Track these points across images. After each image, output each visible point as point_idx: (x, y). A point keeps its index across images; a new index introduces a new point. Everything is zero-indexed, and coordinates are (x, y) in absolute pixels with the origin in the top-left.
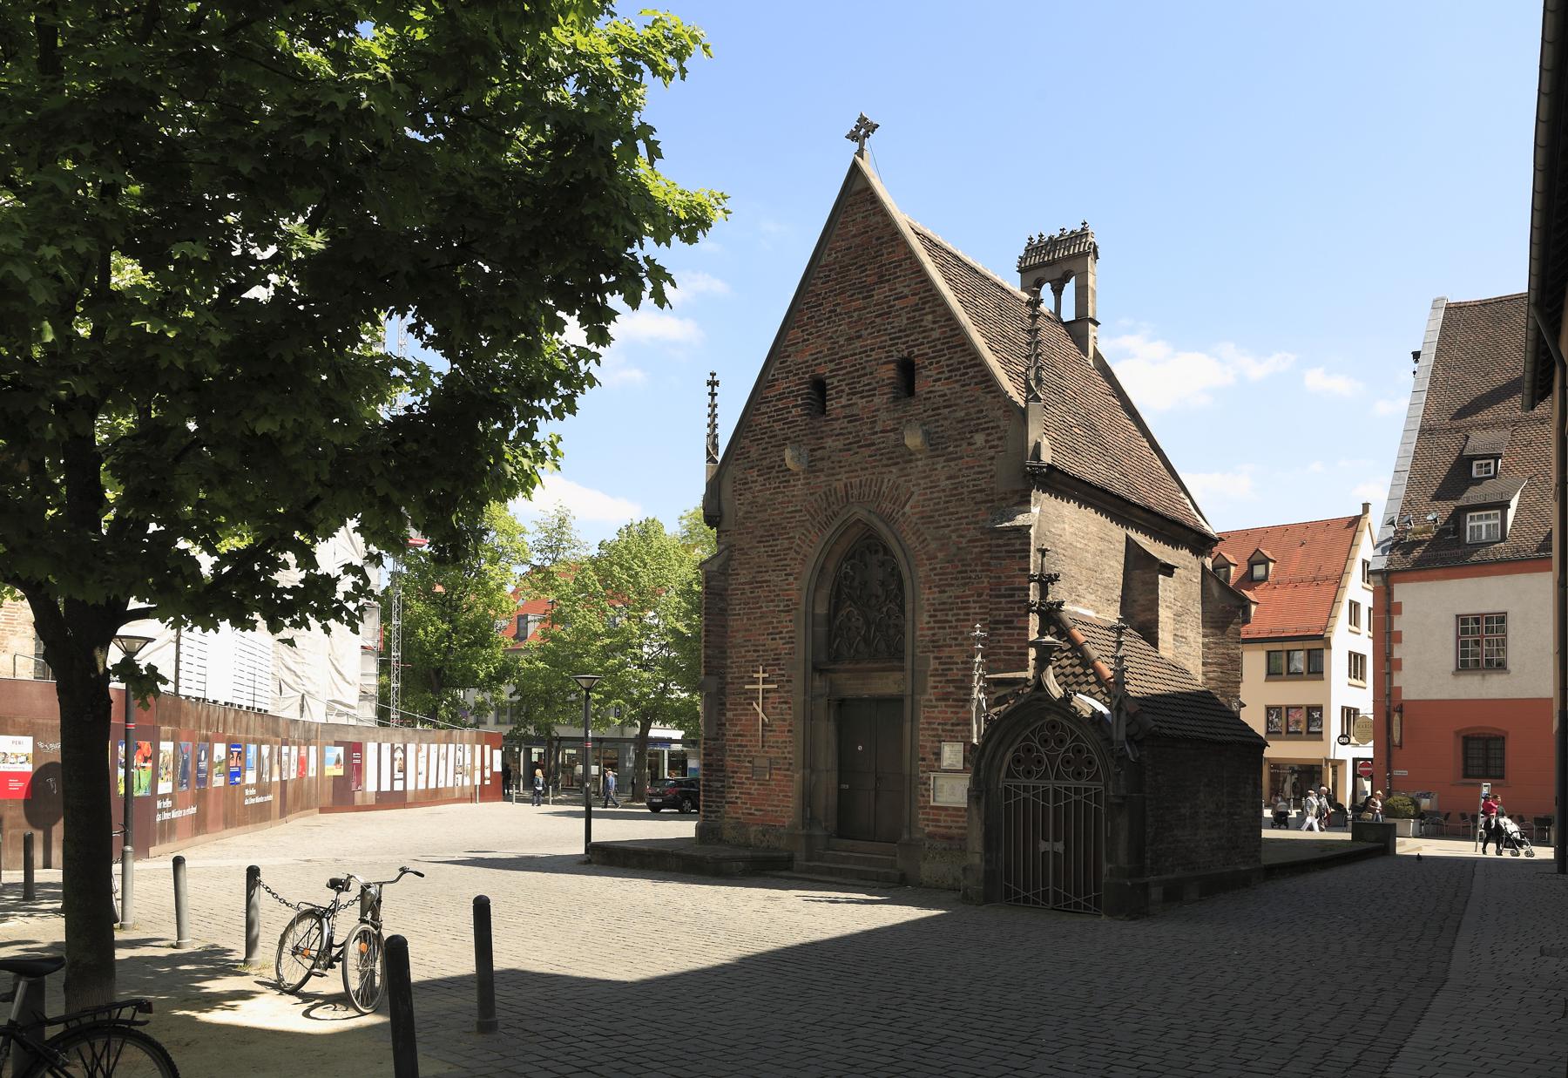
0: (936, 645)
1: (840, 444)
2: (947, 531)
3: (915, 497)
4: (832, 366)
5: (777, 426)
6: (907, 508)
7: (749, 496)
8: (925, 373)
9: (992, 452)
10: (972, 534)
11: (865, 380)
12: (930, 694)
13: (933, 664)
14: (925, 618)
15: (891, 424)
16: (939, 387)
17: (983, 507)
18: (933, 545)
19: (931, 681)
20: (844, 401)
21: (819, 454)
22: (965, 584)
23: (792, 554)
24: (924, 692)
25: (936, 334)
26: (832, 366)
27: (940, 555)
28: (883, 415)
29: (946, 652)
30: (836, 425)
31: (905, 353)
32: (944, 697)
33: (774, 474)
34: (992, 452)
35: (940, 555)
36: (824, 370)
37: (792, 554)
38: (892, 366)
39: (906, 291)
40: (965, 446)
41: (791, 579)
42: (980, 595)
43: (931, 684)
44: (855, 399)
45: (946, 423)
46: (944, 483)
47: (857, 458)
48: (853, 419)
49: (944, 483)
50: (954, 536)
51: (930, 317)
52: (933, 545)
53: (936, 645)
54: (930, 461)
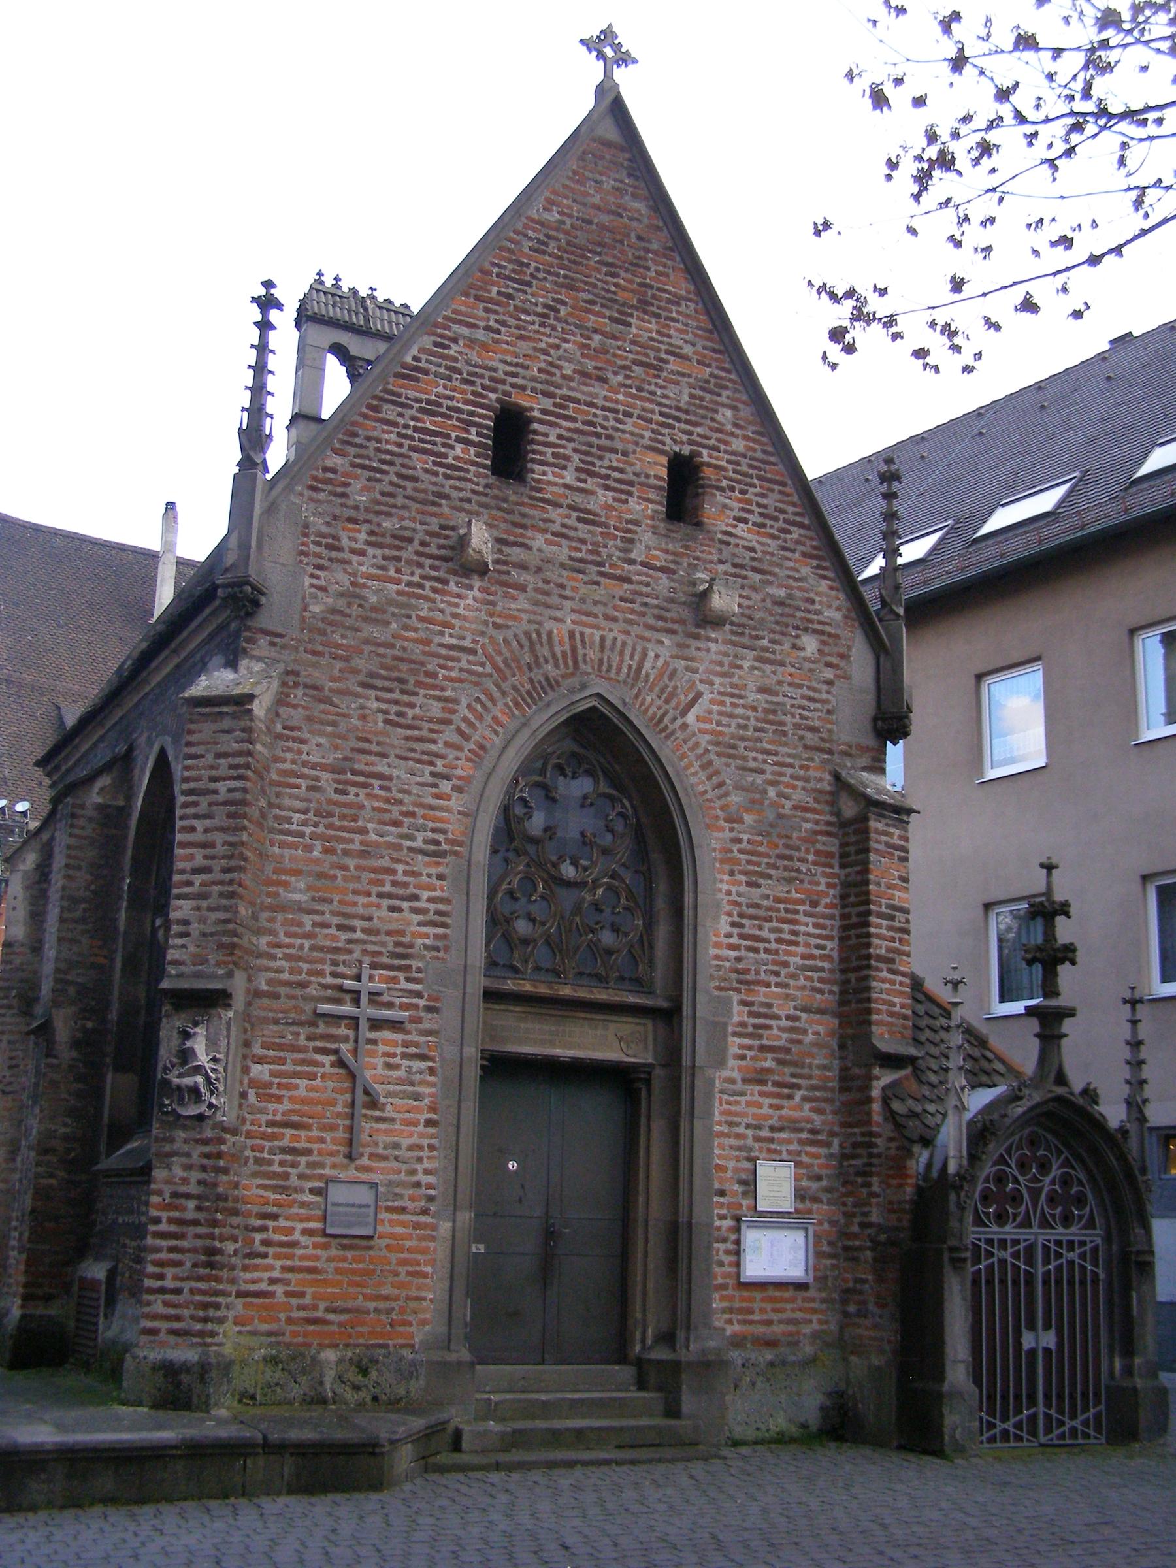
0: (744, 980)
1: (563, 552)
2: (759, 779)
3: (704, 702)
4: (547, 403)
5: (419, 462)
6: (691, 718)
7: (345, 579)
8: (720, 498)
9: (829, 674)
10: (799, 796)
11: (615, 460)
12: (732, 1070)
13: (738, 1014)
14: (724, 925)
15: (661, 560)
16: (741, 530)
17: (818, 757)
18: (736, 798)
19: (734, 1045)
20: (569, 477)
21: (516, 553)
22: (790, 881)
23: (449, 735)
24: (721, 1063)
25: (738, 445)
26: (547, 403)
27: (748, 818)
28: (646, 538)
29: (761, 995)
30: (553, 513)
31: (686, 450)
32: (758, 1078)
33: (408, 553)
34: (829, 674)
35: (748, 818)
36: (535, 405)
37: (449, 735)
38: (664, 460)
39: (687, 350)
40: (787, 646)
41: (446, 786)
42: (814, 904)
43: (734, 1050)
44: (591, 483)
45: (753, 595)
46: (753, 697)
47: (600, 593)
48: (588, 518)
49: (753, 697)
50: (772, 792)
51: (729, 413)
52: (736, 798)
53: (744, 980)
54: (730, 649)
